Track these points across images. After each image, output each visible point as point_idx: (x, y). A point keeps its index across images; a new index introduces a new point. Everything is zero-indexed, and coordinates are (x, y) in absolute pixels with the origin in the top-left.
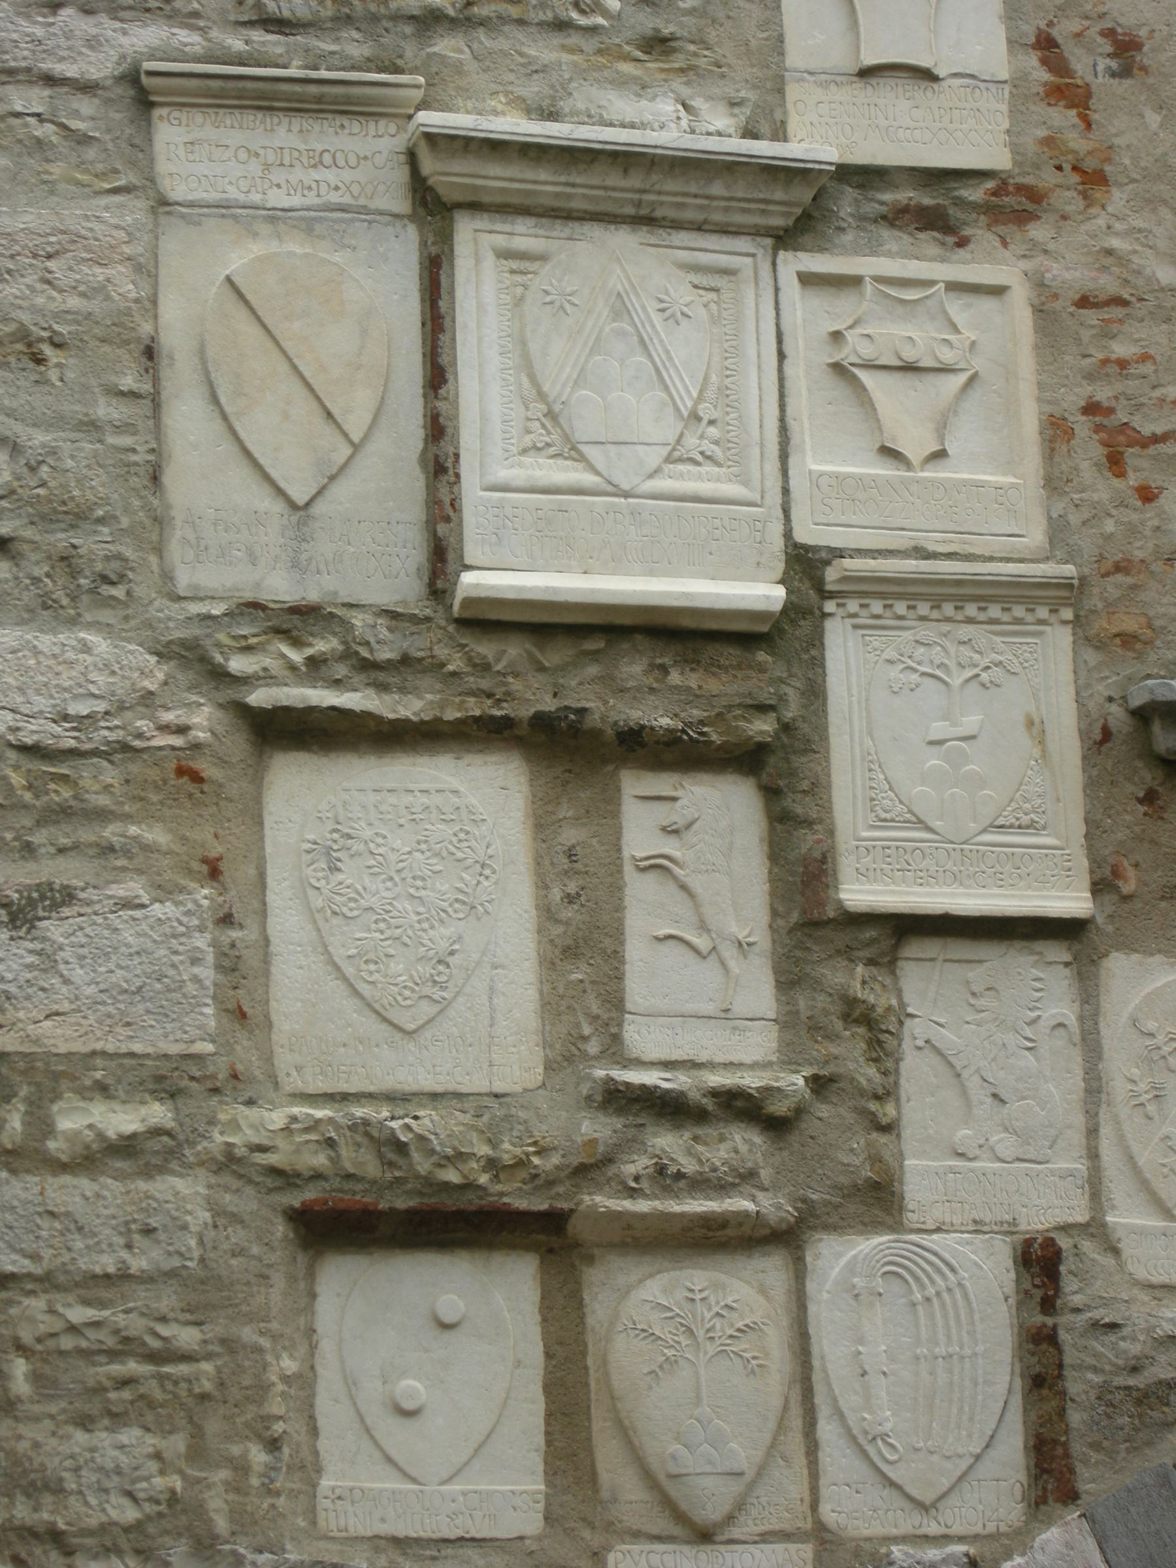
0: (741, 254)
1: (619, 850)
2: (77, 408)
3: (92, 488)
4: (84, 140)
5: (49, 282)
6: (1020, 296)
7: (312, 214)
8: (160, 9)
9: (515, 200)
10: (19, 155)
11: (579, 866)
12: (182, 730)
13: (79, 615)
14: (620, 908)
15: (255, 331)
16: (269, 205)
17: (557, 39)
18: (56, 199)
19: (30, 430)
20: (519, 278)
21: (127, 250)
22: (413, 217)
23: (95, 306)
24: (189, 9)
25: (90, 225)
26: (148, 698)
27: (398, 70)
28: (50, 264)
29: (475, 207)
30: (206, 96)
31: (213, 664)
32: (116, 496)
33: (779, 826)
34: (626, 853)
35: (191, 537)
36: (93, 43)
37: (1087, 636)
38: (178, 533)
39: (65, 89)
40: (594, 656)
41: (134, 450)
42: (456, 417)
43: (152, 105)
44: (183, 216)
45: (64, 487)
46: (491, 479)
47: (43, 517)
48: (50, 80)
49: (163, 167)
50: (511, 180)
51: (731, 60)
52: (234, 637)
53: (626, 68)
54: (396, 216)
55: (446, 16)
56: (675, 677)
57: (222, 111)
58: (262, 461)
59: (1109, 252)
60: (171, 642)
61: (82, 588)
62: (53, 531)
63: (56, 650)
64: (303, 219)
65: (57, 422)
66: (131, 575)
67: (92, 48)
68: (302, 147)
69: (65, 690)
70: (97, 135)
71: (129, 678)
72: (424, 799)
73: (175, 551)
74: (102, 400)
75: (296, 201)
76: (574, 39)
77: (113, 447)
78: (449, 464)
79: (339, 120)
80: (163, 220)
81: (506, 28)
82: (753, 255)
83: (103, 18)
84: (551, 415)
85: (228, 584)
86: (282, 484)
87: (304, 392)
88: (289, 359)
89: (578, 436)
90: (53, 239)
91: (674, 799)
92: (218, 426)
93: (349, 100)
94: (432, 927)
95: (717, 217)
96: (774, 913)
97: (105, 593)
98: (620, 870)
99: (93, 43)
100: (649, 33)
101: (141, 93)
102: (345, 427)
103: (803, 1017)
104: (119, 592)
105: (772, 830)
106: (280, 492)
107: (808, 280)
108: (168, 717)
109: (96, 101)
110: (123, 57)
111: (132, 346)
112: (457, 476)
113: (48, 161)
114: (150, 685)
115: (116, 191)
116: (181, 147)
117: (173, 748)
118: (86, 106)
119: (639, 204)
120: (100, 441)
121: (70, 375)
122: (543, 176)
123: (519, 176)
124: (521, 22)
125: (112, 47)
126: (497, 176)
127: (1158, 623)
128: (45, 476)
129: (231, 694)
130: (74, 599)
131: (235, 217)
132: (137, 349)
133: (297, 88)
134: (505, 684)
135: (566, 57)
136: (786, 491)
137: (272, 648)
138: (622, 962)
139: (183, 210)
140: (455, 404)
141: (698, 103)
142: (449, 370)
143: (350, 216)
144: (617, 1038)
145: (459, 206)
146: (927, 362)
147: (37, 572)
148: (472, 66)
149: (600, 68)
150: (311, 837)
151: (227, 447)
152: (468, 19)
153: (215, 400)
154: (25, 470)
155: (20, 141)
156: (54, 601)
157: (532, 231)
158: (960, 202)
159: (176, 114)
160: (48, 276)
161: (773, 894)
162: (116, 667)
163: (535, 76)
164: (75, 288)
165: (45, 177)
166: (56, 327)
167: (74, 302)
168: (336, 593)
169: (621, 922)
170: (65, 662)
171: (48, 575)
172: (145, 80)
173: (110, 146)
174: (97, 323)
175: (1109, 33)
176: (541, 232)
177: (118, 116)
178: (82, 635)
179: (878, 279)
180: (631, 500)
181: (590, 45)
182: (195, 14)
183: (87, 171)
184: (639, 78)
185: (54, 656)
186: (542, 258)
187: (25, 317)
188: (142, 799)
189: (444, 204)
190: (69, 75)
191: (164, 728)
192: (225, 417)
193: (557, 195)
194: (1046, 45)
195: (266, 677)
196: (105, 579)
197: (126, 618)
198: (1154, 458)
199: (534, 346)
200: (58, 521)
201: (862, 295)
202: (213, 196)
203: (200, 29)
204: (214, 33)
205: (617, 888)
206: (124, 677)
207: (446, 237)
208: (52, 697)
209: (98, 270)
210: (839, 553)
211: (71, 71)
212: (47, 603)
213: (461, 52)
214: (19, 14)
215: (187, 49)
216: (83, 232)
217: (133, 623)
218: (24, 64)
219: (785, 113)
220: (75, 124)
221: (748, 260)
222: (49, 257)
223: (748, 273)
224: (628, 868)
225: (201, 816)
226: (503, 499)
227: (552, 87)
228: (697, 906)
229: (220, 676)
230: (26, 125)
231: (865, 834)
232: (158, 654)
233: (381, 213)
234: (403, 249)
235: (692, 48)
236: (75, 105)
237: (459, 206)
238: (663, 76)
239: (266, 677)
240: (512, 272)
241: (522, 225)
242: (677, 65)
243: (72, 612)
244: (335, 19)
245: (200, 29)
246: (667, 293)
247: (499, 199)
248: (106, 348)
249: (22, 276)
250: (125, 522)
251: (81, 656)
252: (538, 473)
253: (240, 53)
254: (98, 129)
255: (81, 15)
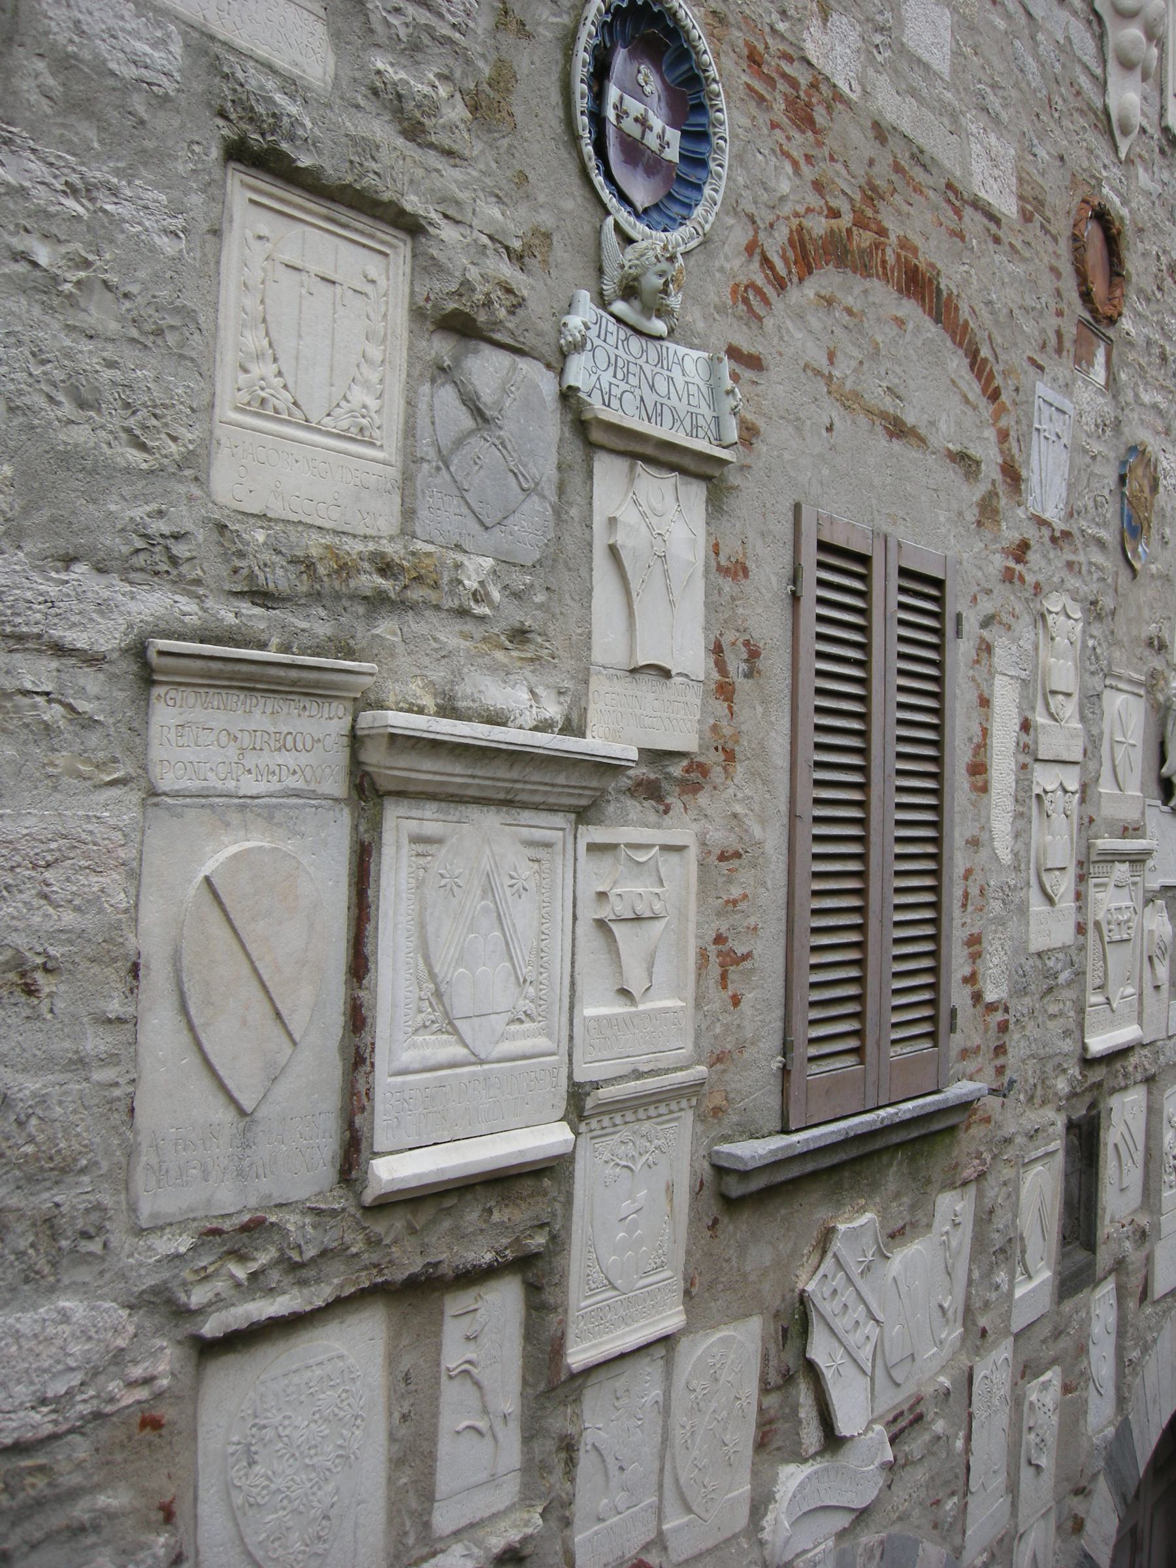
0: (551, 827)
1: (439, 1365)
2: (67, 1044)
3: (78, 1135)
4: (89, 723)
5: (45, 897)
6: (693, 853)
7: (274, 800)
8: (167, 572)
9: (431, 789)
10: (25, 743)
11: (412, 1387)
12: (147, 1381)
13: (58, 1281)
14: (436, 1415)
15: (225, 933)
16: (241, 793)
17: (459, 625)
18: (59, 796)
19: (21, 1078)
20: (421, 861)
21: (122, 853)
22: (347, 801)
23: (88, 922)
24: (193, 576)
25: (90, 827)
26: (119, 1357)
27: (350, 654)
28: (49, 875)
29: (400, 794)
30: (202, 676)
31: (178, 1306)
32: (98, 1140)
33: (534, 1313)
34: (443, 1368)
35: (154, 1161)
36: (104, 607)
37: (700, 1118)
38: (144, 1159)
39: (73, 661)
40: (448, 1211)
41: (117, 1084)
42: (375, 1006)
43: (154, 683)
44: (169, 808)
45: (52, 1140)
46: (397, 1065)
47: (30, 1179)
48: (60, 650)
49: (157, 753)
50: (435, 773)
51: (561, 653)
52: (196, 1272)
53: (499, 655)
54: (336, 800)
55: (389, 598)
56: (496, 1217)
57: (212, 691)
58: (221, 1073)
59: (735, 816)
60: (143, 1292)
61: (61, 1249)
62: (38, 1193)
63: (37, 1328)
64: (266, 806)
65: (48, 1064)
66: (108, 1225)
67: (101, 613)
68: (272, 729)
69: (45, 1371)
70: (101, 718)
71: (104, 1340)
72: (319, 1372)
73: (141, 1179)
74: (90, 1031)
75: (261, 787)
76: (469, 627)
77: (99, 1083)
78: (367, 1055)
79: (306, 702)
80: (151, 811)
81: (427, 613)
82: (563, 829)
83: (114, 579)
84: (438, 994)
85: (184, 1207)
86: (236, 1094)
87: (260, 995)
88: (252, 962)
89: (457, 1013)
90: (53, 845)
91: (476, 1310)
92: (185, 1037)
93: (317, 684)
94: (320, 1488)
95: (551, 800)
96: (525, 1383)
97: (83, 1250)
98: (438, 1383)
99: (104, 607)
100: (518, 625)
101: (145, 669)
102: (290, 1027)
103: (537, 1461)
104: (95, 1246)
105: (528, 1315)
106: (233, 1100)
107: (593, 848)
108: (137, 1372)
109: (101, 676)
110: (131, 626)
111: (119, 964)
112: (372, 1065)
113: (54, 750)
114: (121, 1342)
115: (113, 783)
116: (173, 730)
117: (139, 1402)
118: (91, 680)
119: (508, 791)
120: (87, 1079)
121: (60, 1005)
122: (458, 770)
123: (443, 770)
124: (437, 608)
125: (121, 613)
126: (428, 770)
127: (732, 1095)
128: (33, 1130)
129: (188, 1328)
130: (54, 1264)
131: (212, 806)
132: (124, 966)
133: (282, 673)
134: (389, 1254)
135: (464, 644)
136: (571, 1038)
137: (224, 1271)
138: (435, 1460)
139: (169, 800)
140: (374, 993)
141: (539, 690)
142: (371, 959)
143: (301, 801)
144: (427, 1525)
145: (390, 793)
146: (648, 914)
147: (23, 1244)
148: (401, 649)
149: (482, 655)
150: (235, 1439)
151: (191, 1060)
152: (403, 602)
153: (184, 1009)
154: (14, 1126)
155: (27, 726)
156: (37, 1273)
157: (436, 816)
158: (668, 777)
159: (172, 694)
160: (46, 889)
161: (526, 1367)
162: (92, 1332)
163: (443, 662)
164: (71, 901)
165: (50, 770)
166: (52, 951)
167: (69, 918)
168: (270, 1196)
169: (435, 1426)
170: (46, 1339)
171: (32, 1245)
172: (152, 655)
173: (112, 730)
174: (89, 941)
175: (747, 643)
176: (441, 817)
177: (121, 695)
178: (63, 1304)
179: (629, 846)
180: (486, 1067)
181: (478, 631)
182: (198, 582)
183: (88, 761)
184: (505, 665)
185: (35, 1336)
186: (438, 841)
187: (20, 941)
188: (108, 1463)
189: (377, 791)
190: (79, 646)
191: (131, 1384)
192: (191, 1028)
193: (461, 785)
194: (717, 650)
195: (218, 1302)
196: (86, 1235)
197: (101, 1273)
198: (741, 972)
199: (430, 929)
200: (44, 1180)
201: (617, 859)
202: (195, 785)
203: (199, 597)
204: (209, 603)
205: (434, 1399)
206: (99, 1341)
207: (376, 826)
208: (32, 1383)
209: (94, 879)
210: (596, 1085)
211: (79, 639)
212: (30, 1276)
213: (395, 635)
214: (34, 567)
215: (187, 619)
216: (84, 836)
217: (107, 1276)
218: (36, 630)
219: (587, 702)
220: (82, 706)
221: (560, 833)
222: (48, 865)
223: (560, 846)
224: (444, 1379)
225: (157, 1460)
226: (404, 1083)
227: (453, 672)
228: (482, 1396)
229: (182, 1313)
230: (35, 707)
231: (583, 1304)
232: (131, 1307)
233: (326, 797)
234: (336, 833)
235: (539, 639)
236: (81, 682)
237: (390, 793)
238: (519, 664)
239: (218, 1302)
240: (418, 855)
241: (430, 810)
242: (529, 655)
243: (52, 1279)
244: (309, 595)
245: (199, 597)
246: (515, 870)
247: (420, 789)
248: (96, 969)
249: (20, 891)
250: (105, 1166)
251: (60, 1328)
252: (428, 1052)
253: (231, 626)
254: (103, 711)
255: (94, 572)
